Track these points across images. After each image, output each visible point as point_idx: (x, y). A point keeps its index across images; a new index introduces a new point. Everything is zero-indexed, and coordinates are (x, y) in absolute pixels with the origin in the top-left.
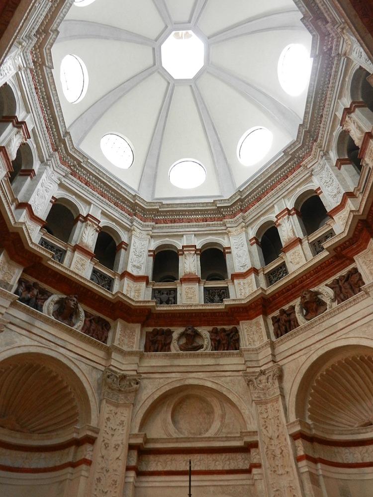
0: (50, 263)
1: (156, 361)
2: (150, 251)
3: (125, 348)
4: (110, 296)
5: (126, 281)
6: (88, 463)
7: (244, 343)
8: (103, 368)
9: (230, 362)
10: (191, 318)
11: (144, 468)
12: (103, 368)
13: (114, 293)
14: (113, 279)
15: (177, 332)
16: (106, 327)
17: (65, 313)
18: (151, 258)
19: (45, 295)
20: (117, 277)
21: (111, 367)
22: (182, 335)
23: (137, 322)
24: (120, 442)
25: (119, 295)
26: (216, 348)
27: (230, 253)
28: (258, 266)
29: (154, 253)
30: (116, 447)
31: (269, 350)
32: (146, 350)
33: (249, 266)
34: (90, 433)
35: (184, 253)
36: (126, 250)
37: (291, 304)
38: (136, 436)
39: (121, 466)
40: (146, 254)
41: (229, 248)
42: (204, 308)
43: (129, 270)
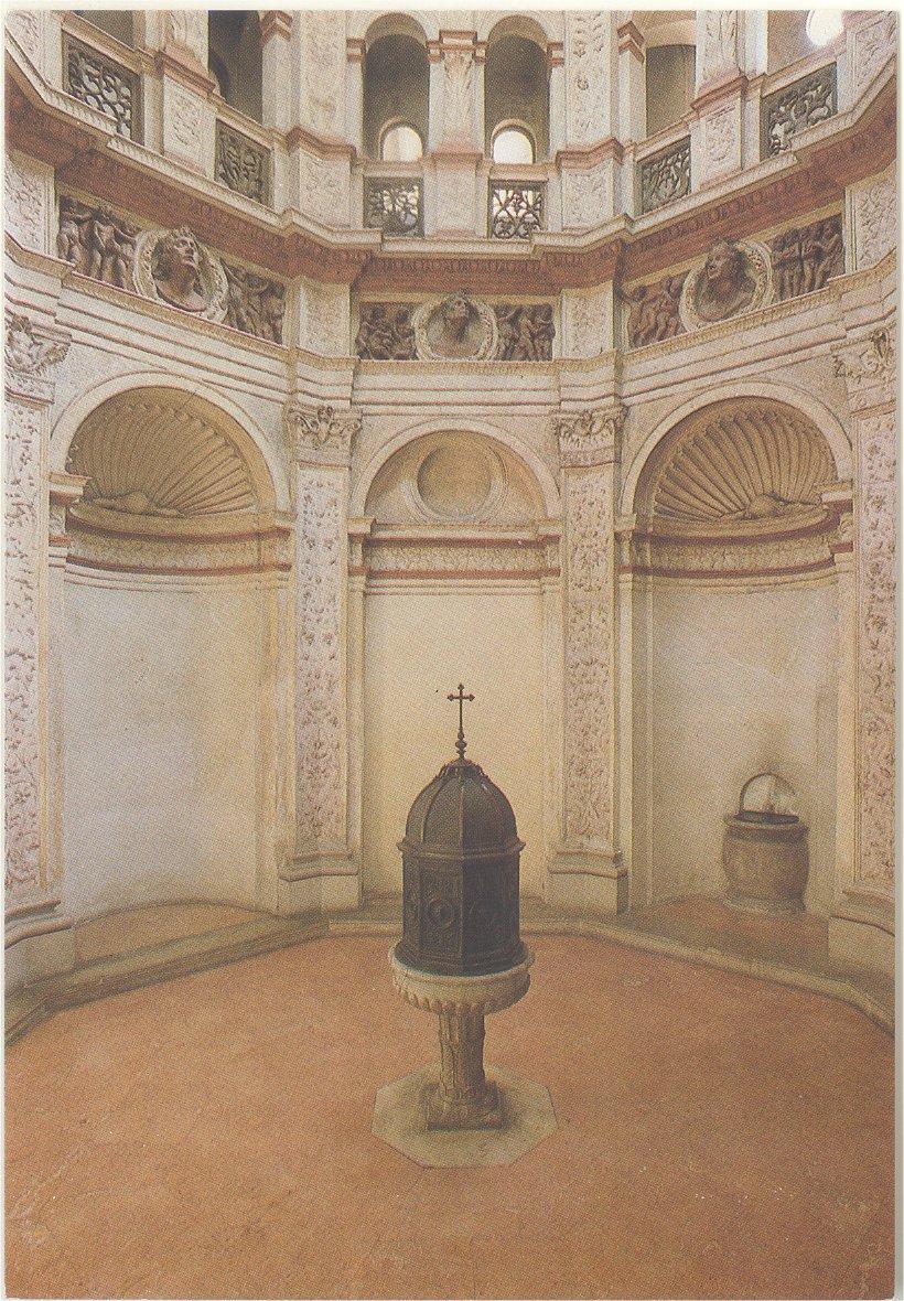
0: (113, 145)
1: (384, 380)
2: (350, 42)
3: (319, 347)
4: (273, 220)
5: (303, 154)
6: (286, 567)
7: (562, 346)
8: (282, 397)
9: (525, 381)
10: (458, 273)
11: (376, 565)
12: (282, 397)
13: (278, 209)
14: (268, 151)
15: (424, 306)
16: (274, 290)
17: (175, 276)
18: (357, 66)
19: (123, 236)
20: (276, 145)
21: (300, 397)
22: (434, 314)
23: (338, 281)
24: (332, 537)
25: (297, 219)
26: (507, 355)
27: (561, 62)
28: (624, 136)
29: (363, 50)
30: (329, 544)
31: (607, 371)
32: (363, 353)
33: (601, 133)
34: (279, 523)
35: (442, 56)
36: (287, 36)
37: (674, 270)
38: (357, 520)
39: (342, 567)
40: (340, 52)
41: (560, 45)
42: (487, 249)
43: (305, 120)
